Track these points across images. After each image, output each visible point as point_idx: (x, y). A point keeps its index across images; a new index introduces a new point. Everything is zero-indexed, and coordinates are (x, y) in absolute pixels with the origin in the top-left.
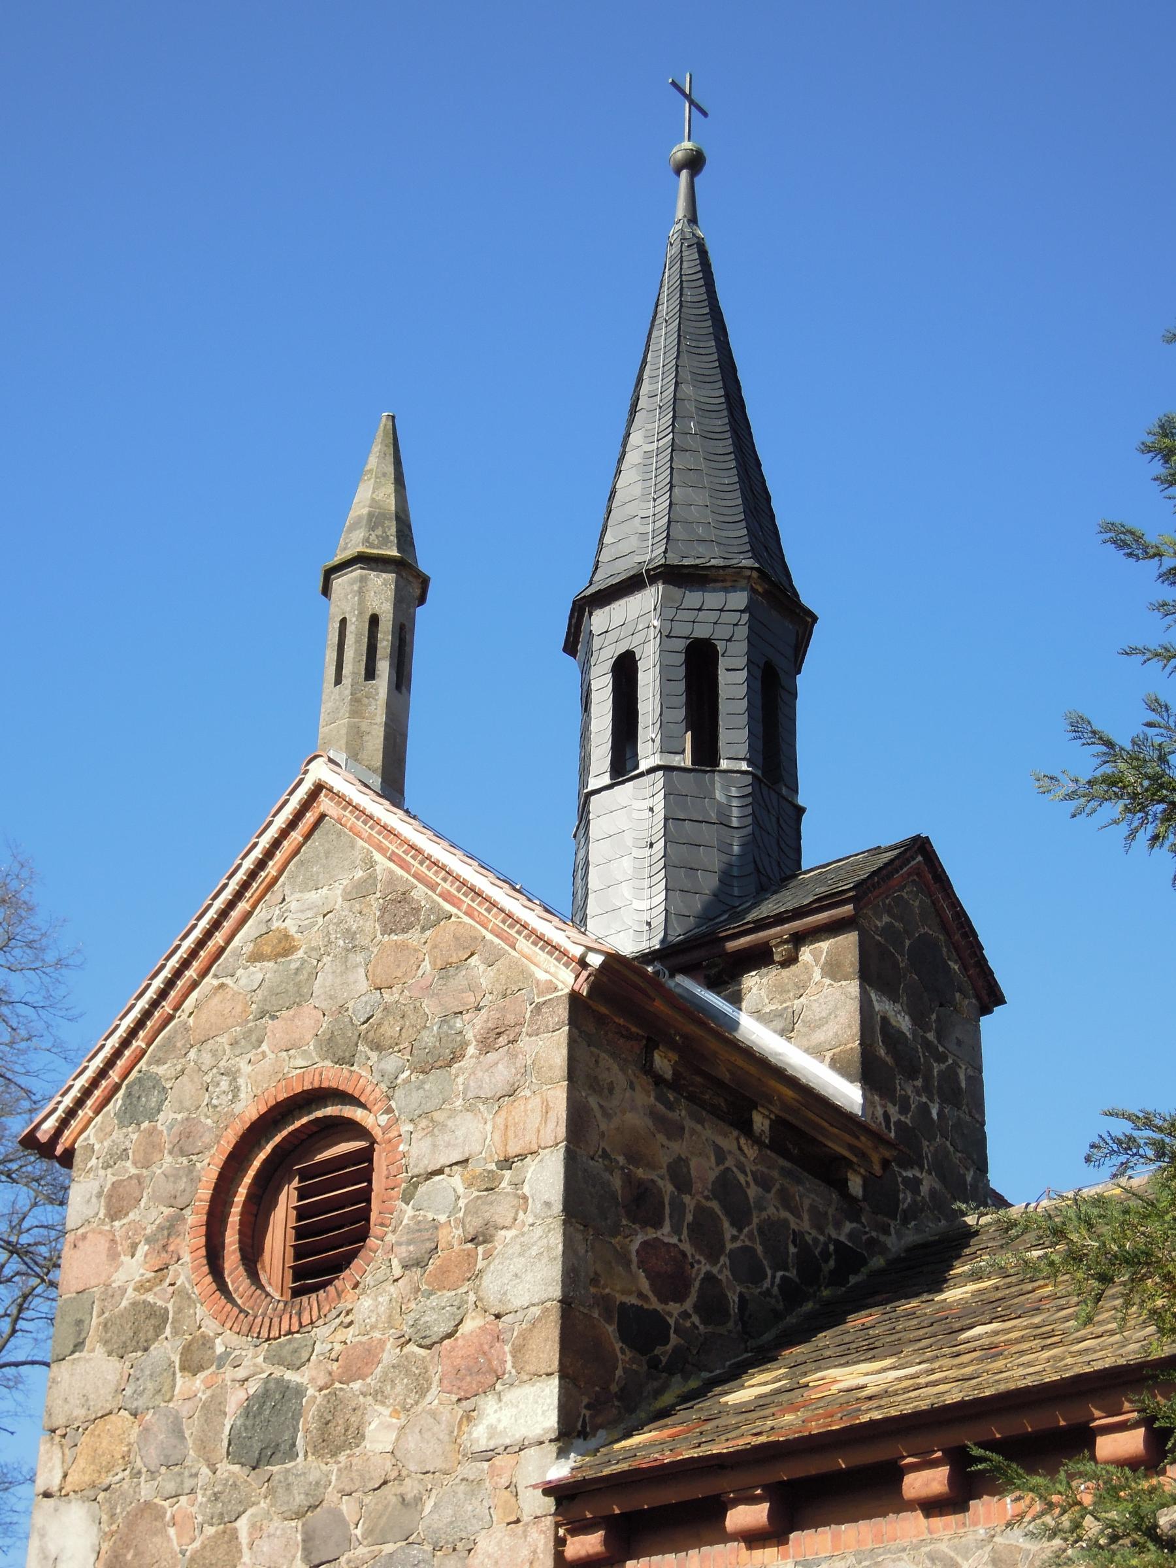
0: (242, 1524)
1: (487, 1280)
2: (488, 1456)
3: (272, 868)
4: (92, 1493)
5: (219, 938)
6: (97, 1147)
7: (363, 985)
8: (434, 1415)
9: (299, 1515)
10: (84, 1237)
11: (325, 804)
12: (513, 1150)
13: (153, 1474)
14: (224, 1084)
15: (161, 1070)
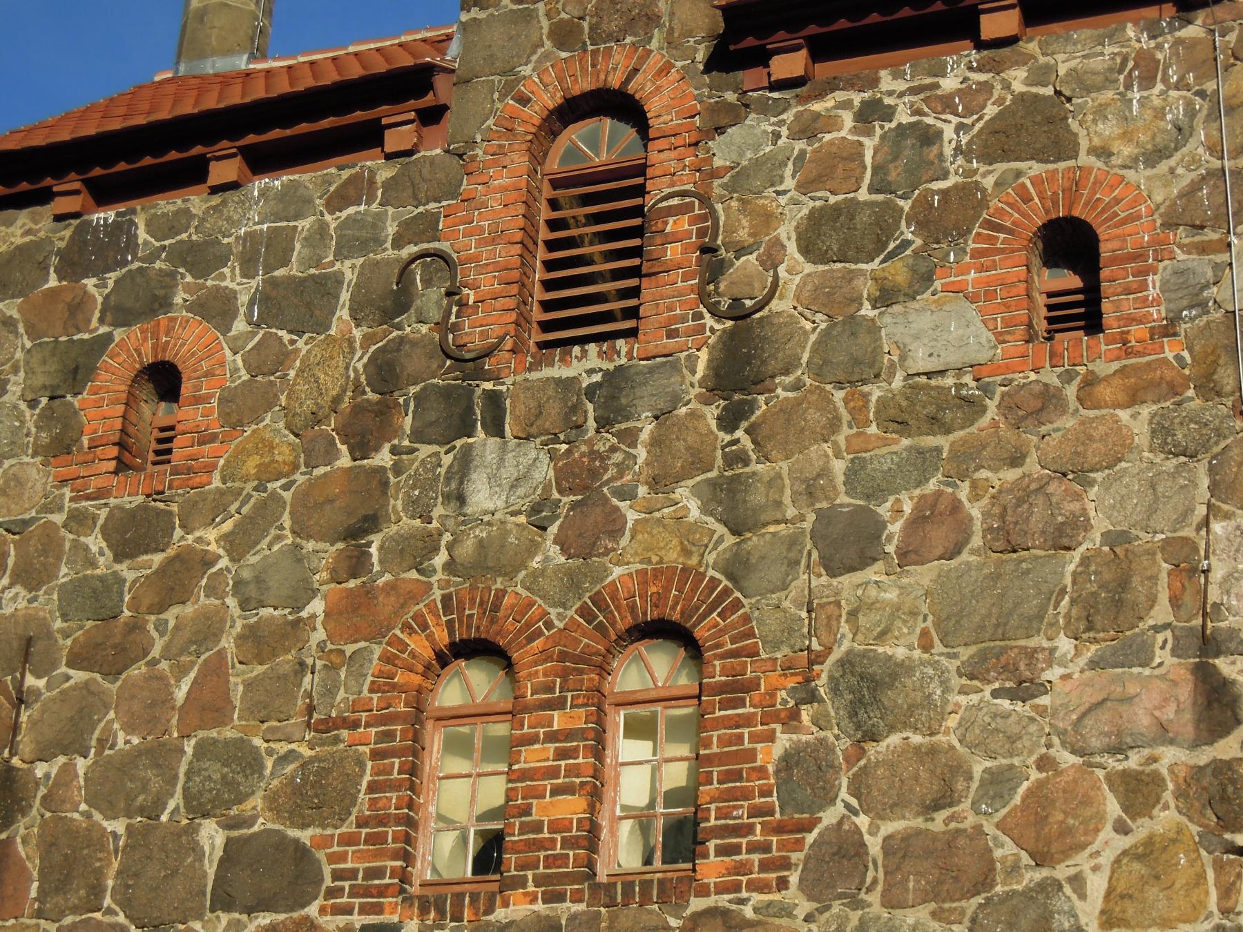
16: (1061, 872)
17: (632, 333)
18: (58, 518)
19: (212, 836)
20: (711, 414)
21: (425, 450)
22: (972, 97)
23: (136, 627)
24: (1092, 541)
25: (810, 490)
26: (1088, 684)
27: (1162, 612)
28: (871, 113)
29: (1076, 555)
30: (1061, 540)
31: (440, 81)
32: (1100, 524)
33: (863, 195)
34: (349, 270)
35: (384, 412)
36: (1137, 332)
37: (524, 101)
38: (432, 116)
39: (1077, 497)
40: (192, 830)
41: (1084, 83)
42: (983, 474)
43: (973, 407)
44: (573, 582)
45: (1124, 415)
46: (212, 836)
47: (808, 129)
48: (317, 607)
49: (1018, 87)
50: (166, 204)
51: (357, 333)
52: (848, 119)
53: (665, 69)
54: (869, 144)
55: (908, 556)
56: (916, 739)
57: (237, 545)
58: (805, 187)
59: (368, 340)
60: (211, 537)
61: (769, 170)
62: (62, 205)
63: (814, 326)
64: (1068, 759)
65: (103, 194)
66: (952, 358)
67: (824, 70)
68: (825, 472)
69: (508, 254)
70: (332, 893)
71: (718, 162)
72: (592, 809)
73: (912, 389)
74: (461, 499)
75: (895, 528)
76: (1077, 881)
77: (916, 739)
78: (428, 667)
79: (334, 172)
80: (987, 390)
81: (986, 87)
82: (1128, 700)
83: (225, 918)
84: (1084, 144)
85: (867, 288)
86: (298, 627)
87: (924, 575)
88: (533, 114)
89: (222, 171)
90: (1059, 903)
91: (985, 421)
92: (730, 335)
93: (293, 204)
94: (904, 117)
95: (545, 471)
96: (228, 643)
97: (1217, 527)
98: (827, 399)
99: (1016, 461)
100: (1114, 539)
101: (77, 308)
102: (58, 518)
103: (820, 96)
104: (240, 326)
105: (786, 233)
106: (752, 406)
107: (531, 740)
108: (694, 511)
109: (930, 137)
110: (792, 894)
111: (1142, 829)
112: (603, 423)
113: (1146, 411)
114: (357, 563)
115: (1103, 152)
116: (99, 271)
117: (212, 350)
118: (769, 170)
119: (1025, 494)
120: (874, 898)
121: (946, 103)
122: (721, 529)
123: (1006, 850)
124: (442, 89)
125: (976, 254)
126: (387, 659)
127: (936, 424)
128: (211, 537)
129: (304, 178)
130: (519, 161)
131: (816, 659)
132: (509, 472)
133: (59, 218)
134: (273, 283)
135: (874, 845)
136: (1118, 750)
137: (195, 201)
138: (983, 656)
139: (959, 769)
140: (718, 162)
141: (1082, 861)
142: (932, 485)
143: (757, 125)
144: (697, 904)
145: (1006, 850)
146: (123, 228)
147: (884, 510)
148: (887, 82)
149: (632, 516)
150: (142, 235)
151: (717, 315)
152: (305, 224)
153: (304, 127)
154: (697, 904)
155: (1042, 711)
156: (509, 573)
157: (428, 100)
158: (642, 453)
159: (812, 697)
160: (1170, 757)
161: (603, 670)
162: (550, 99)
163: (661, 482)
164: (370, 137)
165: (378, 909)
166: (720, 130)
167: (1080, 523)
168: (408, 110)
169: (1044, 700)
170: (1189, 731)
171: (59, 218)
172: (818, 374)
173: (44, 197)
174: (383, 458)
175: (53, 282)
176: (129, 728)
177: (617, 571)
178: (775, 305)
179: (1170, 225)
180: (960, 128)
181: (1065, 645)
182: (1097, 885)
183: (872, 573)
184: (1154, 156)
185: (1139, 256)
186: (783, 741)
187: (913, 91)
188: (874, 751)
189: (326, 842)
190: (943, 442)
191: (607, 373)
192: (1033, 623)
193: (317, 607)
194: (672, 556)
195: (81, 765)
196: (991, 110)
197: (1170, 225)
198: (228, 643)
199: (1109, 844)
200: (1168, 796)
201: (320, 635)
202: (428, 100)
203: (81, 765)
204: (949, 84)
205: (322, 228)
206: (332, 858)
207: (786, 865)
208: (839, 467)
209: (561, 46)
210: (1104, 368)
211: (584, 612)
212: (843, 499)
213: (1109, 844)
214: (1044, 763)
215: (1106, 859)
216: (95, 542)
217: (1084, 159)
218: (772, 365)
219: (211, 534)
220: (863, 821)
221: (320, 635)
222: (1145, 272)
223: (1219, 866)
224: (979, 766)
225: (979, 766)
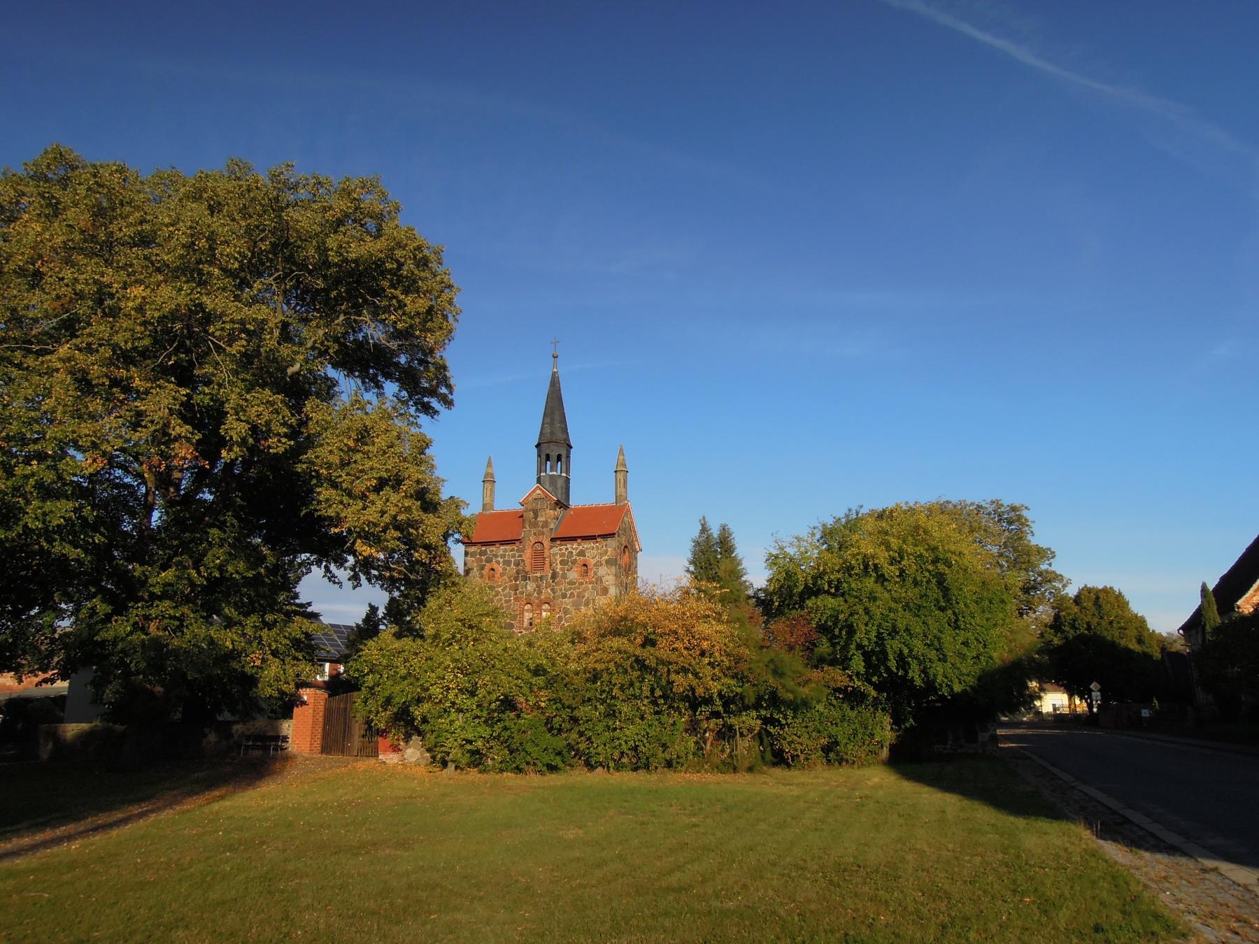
22: (577, 549)
25: (561, 590)
28: (567, 549)
30: (584, 597)
34: (513, 560)
44: (538, 598)
57: (503, 590)
60: (500, 589)
61: (556, 554)
69: (529, 560)
86: (510, 600)
87: (571, 600)
93: (505, 551)
101: (481, 560)
109: (572, 553)
114: (516, 594)
118: (556, 554)
119: (580, 592)
128: (500, 589)
129: (507, 547)
146: (486, 550)
163: (546, 588)
184: (593, 558)
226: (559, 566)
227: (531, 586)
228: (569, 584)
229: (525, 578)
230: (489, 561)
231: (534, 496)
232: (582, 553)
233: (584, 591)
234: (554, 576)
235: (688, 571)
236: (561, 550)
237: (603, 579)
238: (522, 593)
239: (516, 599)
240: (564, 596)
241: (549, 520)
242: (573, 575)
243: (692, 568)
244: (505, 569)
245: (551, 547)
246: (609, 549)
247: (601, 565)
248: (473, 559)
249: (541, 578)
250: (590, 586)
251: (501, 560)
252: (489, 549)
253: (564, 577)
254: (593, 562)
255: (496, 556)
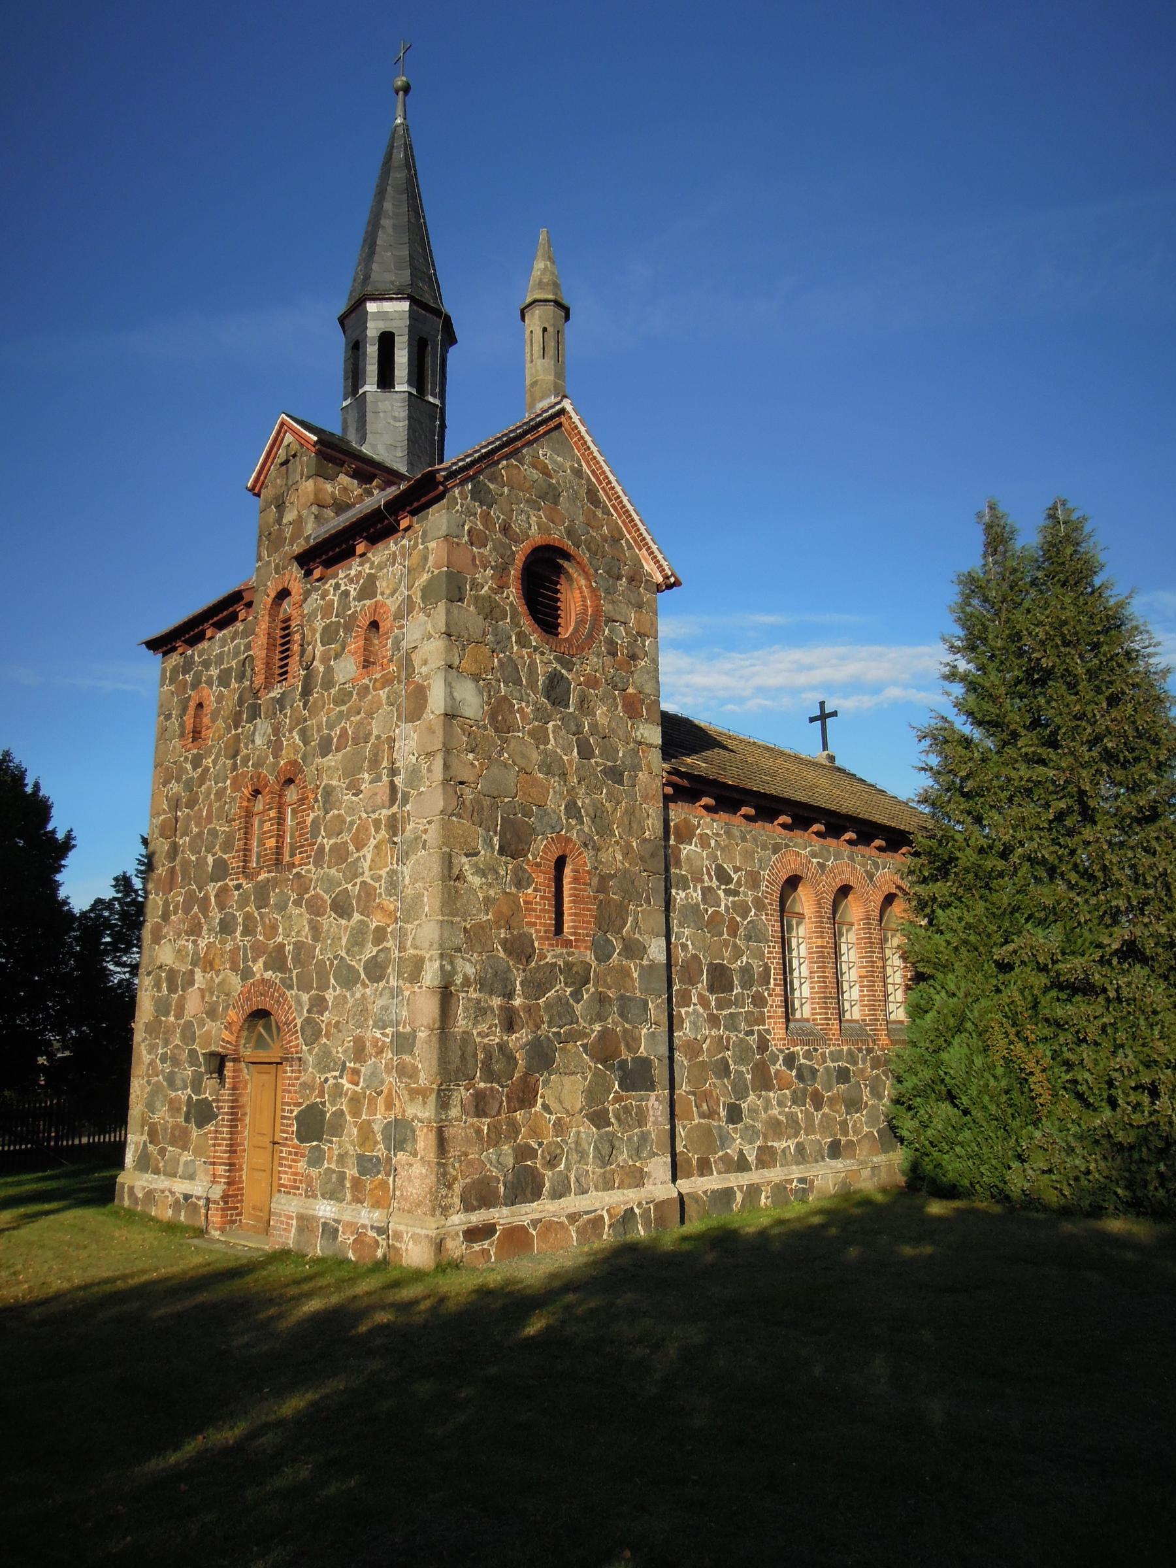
0: (550, 725)
1: (635, 676)
2: (640, 744)
3: (542, 430)
4: (476, 678)
5: (519, 444)
6: (459, 501)
7: (582, 518)
8: (621, 718)
9: (574, 735)
10: (458, 544)
11: (563, 419)
12: (642, 631)
13: (506, 685)
14: (524, 517)
15: (492, 486)
16: (361, 854)
17: (286, 679)
18: (182, 759)
19: (210, 859)
20: (301, 704)
21: (248, 725)
23: (197, 793)
24: (373, 739)
26: (370, 789)
27: (385, 764)
29: (370, 744)
31: (244, 594)
32: (375, 733)
33: (334, 619)
34: (234, 664)
35: (240, 713)
36: (385, 661)
37: (268, 596)
38: (249, 605)
39: (370, 724)
40: (206, 857)
41: (380, 567)
42: (352, 718)
43: (351, 693)
45: (381, 692)
46: (210, 859)
47: (323, 598)
48: (228, 782)
49: (368, 571)
50: (200, 646)
51: (236, 686)
52: (332, 589)
53: (296, 579)
54: (336, 599)
55: (338, 750)
56: (336, 812)
57: (215, 763)
58: (322, 619)
59: (239, 688)
61: (313, 615)
62: (180, 650)
63: (321, 669)
64: (364, 815)
65: (193, 642)
66: (348, 677)
67: (330, 571)
68: (322, 723)
70: (231, 874)
71: (305, 612)
72: (277, 842)
73: (340, 689)
74: (253, 741)
75: (335, 740)
76: (364, 856)
77: (336, 812)
78: (249, 799)
79: (231, 629)
80: (354, 688)
81: (360, 572)
82: (376, 794)
83: (212, 884)
84: (379, 591)
85: (332, 653)
86: (225, 788)
87: (340, 755)
88: (270, 600)
89: (208, 634)
90: (360, 864)
91: (353, 699)
92: (305, 675)
93: (224, 643)
94: (343, 588)
95: (270, 731)
96: (212, 796)
97: (397, 731)
98: (323, 695)
99: (359, 713)
100: (378, 737)
102: (182, 759)
103: (326, 583)
104: (214, 688)
105: (318, 636)
106: (308, 700)
107: (266, 821)
108: (297, 737)
109: (346, 594)
110: (311, 867)
111: (379, 837)
112: (281, 712)
113: (386, 690)
115: (382, 594)
116: (188, 672)
117: (209, 696)
119: (360, 723)
120: (325, 866)
121: (351, 581)
122: (302, 745)
123: (351, 847)
124: (247, 597)
125: (355, 637)
126: (241, 798)
127: (344, 703)
130: (267, 618)
131: (318, 787)
132: (263, 731)
133: (181, 654)
134: (221, 671)
135: (327, 848)
136: (374, 811)
137: (205, 645)
138: (350, 783)
139: (344, 822)
140: (305, 612)
141: (365, 849)
142: (343, 724)
143: (315, 596)
144: (295, 871)
145: (351, 847)
147: (333, 734)
148: (341, 575)
149: (285, 743)
150: (196, 658)
151: (304, 670)
152: (226, 649)
153: (225, 613)
154: (295, 871)
155: (360, 799)
156: (262, 766)
157: (245, 601)
158: (288, 721)
159: (316, 801)
160: (385, 812)
161: (280, 796)
162: (273, 594)
164: (233, 618)
165: (238, 879)
166: (306, 599)
167: (370, 733)
168: (239, 607)
169: (361, 796)
170: (387, 804)
171: (181, 654)
172: (322, 688)
173: (174, 649)
174: (240, 730)
175: (181, 677)
176: (196, 827)
177: (282, 762)
178: (315, 663)
179: (394, 620)
180: (355, 589)
181: (366, 776)
182: (369, 857)
183: (330, 757)
185: (387, 633)
186: (312, 815)
187: (345, 577)
188: (328, 816)
189: (230, 857)
190: (344, 708)
191: (282, 694)
192: (360, 770)
193: (228, 782)
194: (292, 757)
195: (187, 838)
196: (362, 581)
197: (394, 620)
198: (212, 796)
199: (373, 842)
200: (383, 826)
201: (229, 791)
202: (245, 601)
203: (187, 838)
204: (353, 573)
205: (229, 648)
206: (232, 863)
207: (309, 857)
208: (325, 719)
209: (276, 573)
210: (378, 676)
211: (276, 777)
212: (325, 731)
213: (373, 842)
214: (360, 818)
215: (371, 849)
216: (189, 766)
217: (379, 597)
218: (313, 686)
219: (210, 760)
220: (325, 840)
221: (229, 791)
222: (387, 639)
223: (391, 848)
224: (348, 819)
225: (348, 819)
226: (320, 649)
227: (262, 729)
228: (336, 703)
229: (255, 713)
230: (196, 685)
231: (282, 454)
232: (368, 589)
233: (370, 715)
234: (306, 692)
235: (952, 676)
236: (323, 598)
237: (416, 658)
238: (246, 760)
239: (236, 786)
240: (325, 748)
241: (305, 512)
242: (346, 669)
243: (963, 665)
244: (220, 698)
245: (307, 594)
246: (432, 545)
247: (411, 608)
248: (172, 688)
249: (281, 702)
250: (383, 694)
251: (214, 672)
252: (195, 653)
253: (328, 683)
254: (392, 604)
255: (206, 664)
